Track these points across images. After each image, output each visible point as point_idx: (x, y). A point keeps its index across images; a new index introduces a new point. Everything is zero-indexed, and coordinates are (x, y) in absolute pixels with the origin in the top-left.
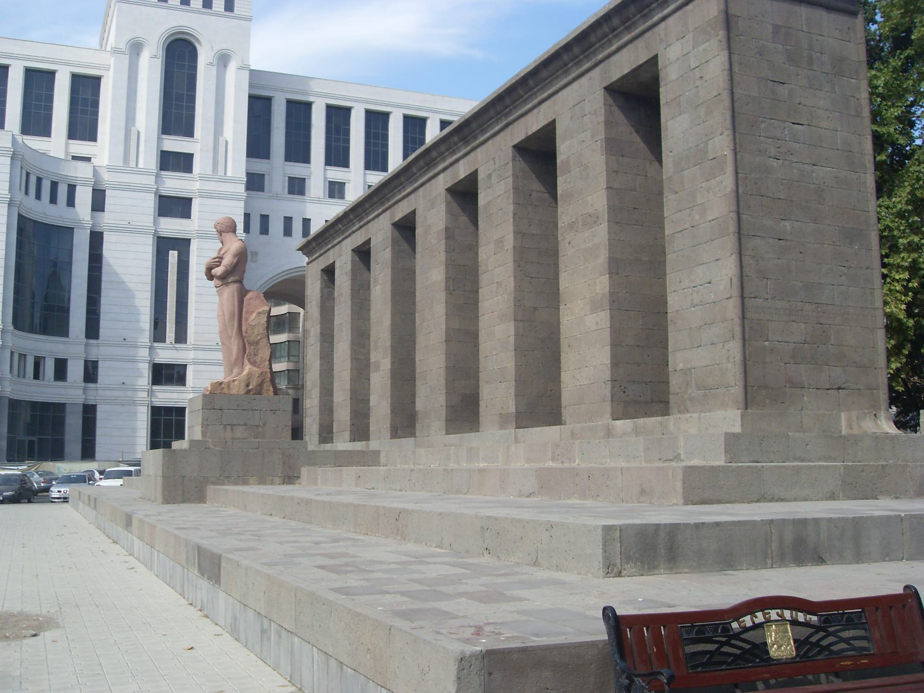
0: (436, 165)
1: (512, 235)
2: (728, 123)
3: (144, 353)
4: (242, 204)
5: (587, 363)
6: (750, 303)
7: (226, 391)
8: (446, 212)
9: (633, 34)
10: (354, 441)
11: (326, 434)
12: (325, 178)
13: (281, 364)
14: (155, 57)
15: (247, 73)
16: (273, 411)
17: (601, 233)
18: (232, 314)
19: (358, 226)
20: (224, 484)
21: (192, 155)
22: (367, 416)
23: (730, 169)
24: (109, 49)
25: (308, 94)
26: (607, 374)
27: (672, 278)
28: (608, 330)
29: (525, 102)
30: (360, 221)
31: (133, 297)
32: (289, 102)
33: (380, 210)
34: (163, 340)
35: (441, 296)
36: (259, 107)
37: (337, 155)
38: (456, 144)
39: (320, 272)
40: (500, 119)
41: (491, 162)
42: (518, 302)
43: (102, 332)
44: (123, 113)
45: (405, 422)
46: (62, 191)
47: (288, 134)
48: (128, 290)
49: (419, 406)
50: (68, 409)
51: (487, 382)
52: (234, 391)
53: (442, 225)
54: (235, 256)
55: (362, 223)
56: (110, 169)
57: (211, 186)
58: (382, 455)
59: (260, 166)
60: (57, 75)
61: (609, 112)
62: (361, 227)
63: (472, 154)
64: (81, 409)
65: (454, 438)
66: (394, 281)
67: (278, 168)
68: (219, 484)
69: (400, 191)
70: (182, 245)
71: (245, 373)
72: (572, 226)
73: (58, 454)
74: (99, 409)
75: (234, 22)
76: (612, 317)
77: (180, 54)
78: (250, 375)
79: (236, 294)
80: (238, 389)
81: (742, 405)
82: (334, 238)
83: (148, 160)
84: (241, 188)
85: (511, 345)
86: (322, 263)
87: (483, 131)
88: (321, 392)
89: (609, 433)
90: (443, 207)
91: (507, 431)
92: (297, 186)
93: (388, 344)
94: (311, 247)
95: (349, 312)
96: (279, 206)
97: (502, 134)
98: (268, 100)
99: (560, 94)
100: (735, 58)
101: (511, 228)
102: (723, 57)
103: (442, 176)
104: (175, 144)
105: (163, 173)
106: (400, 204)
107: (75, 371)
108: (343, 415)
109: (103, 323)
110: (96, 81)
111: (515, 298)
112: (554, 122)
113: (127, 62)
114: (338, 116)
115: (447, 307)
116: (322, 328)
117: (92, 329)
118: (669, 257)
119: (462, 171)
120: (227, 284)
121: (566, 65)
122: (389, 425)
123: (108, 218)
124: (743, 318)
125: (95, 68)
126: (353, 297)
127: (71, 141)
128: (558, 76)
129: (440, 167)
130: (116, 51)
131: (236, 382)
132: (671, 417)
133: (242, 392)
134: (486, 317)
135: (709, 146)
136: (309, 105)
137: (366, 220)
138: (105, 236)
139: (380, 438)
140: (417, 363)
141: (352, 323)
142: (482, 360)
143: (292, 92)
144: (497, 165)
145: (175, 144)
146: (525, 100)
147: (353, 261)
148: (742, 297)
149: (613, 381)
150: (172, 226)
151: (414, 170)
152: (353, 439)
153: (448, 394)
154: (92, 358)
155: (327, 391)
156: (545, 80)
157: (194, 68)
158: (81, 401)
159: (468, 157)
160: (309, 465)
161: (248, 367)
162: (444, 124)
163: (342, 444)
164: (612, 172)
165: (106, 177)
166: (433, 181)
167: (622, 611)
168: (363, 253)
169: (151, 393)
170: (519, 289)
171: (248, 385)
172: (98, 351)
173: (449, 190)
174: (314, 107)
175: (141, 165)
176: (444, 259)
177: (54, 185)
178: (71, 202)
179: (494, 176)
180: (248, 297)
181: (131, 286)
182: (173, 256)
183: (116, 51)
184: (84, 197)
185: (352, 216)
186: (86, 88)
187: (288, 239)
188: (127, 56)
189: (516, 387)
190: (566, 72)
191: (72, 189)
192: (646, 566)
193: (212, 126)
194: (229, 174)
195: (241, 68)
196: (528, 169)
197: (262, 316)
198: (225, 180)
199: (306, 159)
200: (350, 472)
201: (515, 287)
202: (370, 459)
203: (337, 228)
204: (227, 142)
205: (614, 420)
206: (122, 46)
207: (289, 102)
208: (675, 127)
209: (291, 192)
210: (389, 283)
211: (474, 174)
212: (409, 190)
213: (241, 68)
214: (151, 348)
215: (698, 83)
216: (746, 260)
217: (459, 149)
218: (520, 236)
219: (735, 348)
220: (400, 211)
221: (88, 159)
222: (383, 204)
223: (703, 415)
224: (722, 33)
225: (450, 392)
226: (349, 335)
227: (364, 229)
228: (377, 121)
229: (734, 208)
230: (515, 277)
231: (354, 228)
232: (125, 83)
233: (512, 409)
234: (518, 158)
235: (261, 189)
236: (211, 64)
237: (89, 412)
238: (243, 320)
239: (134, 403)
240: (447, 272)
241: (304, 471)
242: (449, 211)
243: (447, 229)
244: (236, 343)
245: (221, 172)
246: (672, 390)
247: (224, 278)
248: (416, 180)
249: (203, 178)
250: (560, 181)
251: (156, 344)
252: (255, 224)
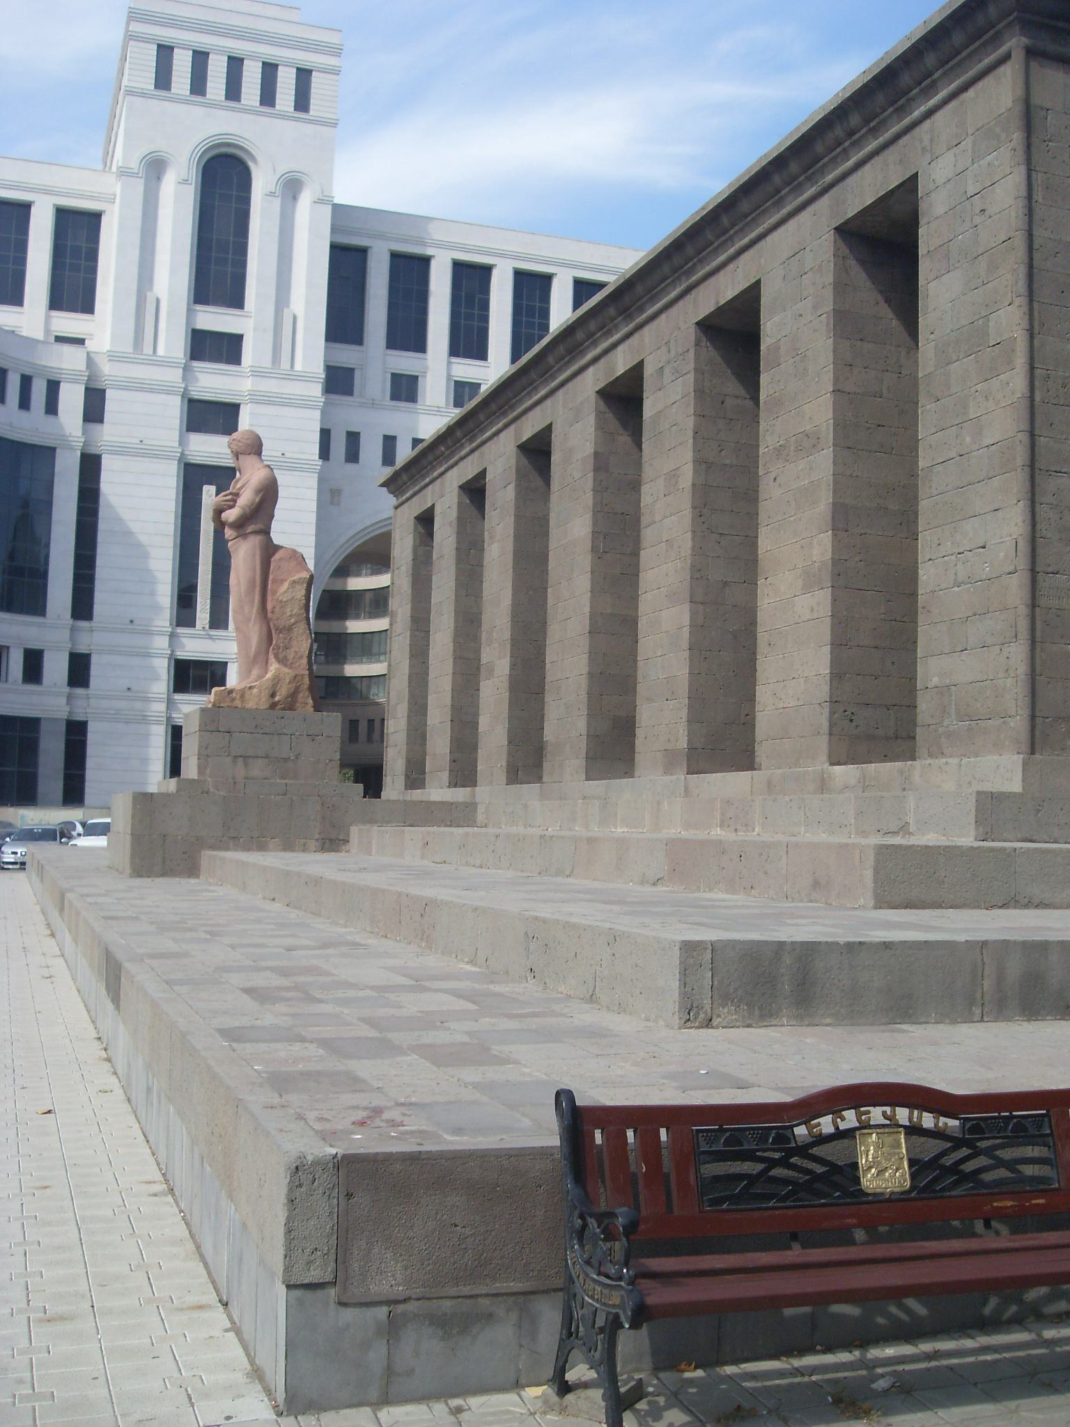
0: (582, 353)
1: (690, 465)
2: (1022, 286)
3: (162, 643)
4: (317, 415)
5: (795, 674)
6: (1045, 582)
7: (238, 703)
8: (597, 429)
9: (881, 140)
10: (455, 786)
11: (416, 776)
12: (449, 377)
13: (379, 665)
14: (185, 182)
15: (328, 210)
16: (312, 737)
17: (822, 464)
18: (252, 583)
19: (468, 449)
20: (227, 849)
21: (239, 338)
22: (474, 748)
23: (1021, 360)
24: (114, 169)
25: (424, 244)
26: (823, 691)
27: (926, 538)
28: (829, 620)
29: (716, 252)
30: (471, 441)
31: (145, 556)
32: (395, 256)
33: (500, 425)
34: (191, 623)
35: (585, 561)
36: (347, 263)
37: (469, 339)
38: (613, 319)
39: (412, 521)
40: (679, 278)
41: (664, 349)
42: (698, 573)
43: (98, 609)
44: (134, 270)
45: (528, 761)
46: (39, 392)
47: (392, 306)
48: (139, 545)
49: (549, 734)
50: (44, 727)
51: (648, 699)
52: (251, 705)
53: (589, 449)
54: (258, 491)
55: (474, 444)
56: (113, 357)
57: (270, 386)
58: (481, 809)
59: (347, 355)
60: (33, 210)
61: (841, 270)
62: (472, 451)
63: (636, 336)
64: (64, 728)
65: (597, 786)
66: (517, 537)
67: (376, 359)
68: (220, 849)
69: (529, 395)
71: (269, 675)
72: (780, 451)
73: (27, 795)
74: (91, 728)
75: (309, 129)
76: (834, 601)
77: (224, 177)
78: (277, 680)
79: (258, 552)
80: (257, 701)
81: (1025, 747)
82: (434, 469)
83: (173, 343)
84: (315, 390)
85: (685, 644)
86: (416, 507)
87: (653, 300)
88: (410, 710)
89: (823, 785)
90: (591, 420)
91: (674, 777)
92: (405, 389)
93: (507, 635)
94: (400, 482)
95: (452, 584)
96: (377, 418)
97: (681, 303)
98: (363, 252)
99: (769, 238)
100: (1039, 178)
101: (689, 455)
102: (1017, 178)
103: (591, 370)
104: (215, 319)
105: (196, 364)
106: (531, 414)
107: (56, 668)
108: (439, 745)
109: (98, 596)
110: (94, 219)
111: (693, 566)
112: (758, 282)
113: (141, 189)
114: (471, 280)
115: (592, 580)
116: (413, 609)
117: (83, 606)
118: (923, 505)
119: (621, 362)
120: (244, 536)
121: (778, 191)
122: (504, 764)
123: (109, 433)
124: (1033, 605)
125: (92, 198)
126: (459, 560)
127: (54, 313)
128: (764, 211)
129: (589, 356)
130: (123, 173)
131: (255, 690)
132: (917, 763)
133: (264, 705)
134: (649, 596)
135: (991, 324)
136: (425, 261)
137: (478, 441)
139: (491, 783)
140: (548, 666)
141: (457, 601)
142: (640, 664)
143: (398, 240)
144: (673, 353)
145: (215, 319)
146: (716, 248)
147: (460, 504)
148: (1033, 571)
149: (834, 702)
151: (551, 360)
152: (454, 784)
153: (591, 716)
154: (82, 649)
155: (418, 708)
156: (746, 216)
157: (246, 201)
158: (64, 715)
159: (628, 342)
160: (364, 822)
161: (274, 667)
162: (583, 289)
163: (438, 791)
164: (843, 366)
165: (107, 369)
166: (579, 378)
167: (591, 1095)
168: (475, 491)
169: (170, 703)
170: (699, 551)
171: (273, 695)
172: (91, 639)
173: (602, 393)
174: (434, 265)
175: (161, 351)
176: (590, 503)
177: (26, 381)
178: (52, 407)
179: (667, 371)
180: (277, 556)
181: (143, 539)
183: (123, 173)
184: (72, 400)
185: (459, 434)
186: (78, 231)
188: (142, 181)
189: (690, 707)
190: (779, 203)
191: (53, 388)
192: (757, 1012)
193: (272, 292)
194: (298, 366)
195: (319, 201)
196: (719, 359)
197: (298, 587)
198: (291, 376)
200: (414, 834)
201: (693, 548)
202: (461, 815)
203: (437, 452)
204: (295, 318)
205: (832, 764)
206: (134, 165)
207: (395, 256)
208: (942, 291)
209: (395, 396)
210: (511, 539)
211: (639, 366)
212: (543, 392)
213: (319, 201)
214: (172, 636)
215: (977, 220)
216: (1042, 511)
217: (616, 328)
218: (704, 467)
219: (1018, 654)
220: (529, 427)
221: (81, 342)
222: (505, 414)
223: (965, 760)
224: (1017, 137)
225: (594, 713)
226: (452, 621)
227: (477, 454)
228: (533, 288)
229: (1025, 426)
230: (694, 532)
231: (463, 453)
232: (138, 224)
233: (683, 743)
234: (704, 342)
235: (349, 391)
236: (272, 194)
237: (76, 733)
238: (269, 592)
239: (144, 720)
240: (595, 524)
241: (354, 831)
242: (600, 426)
243: (596, 454)
244: (257, 628)
245: (285, 364)
246: (919, 720)
247: (240, 525)
248: (553, 377)
249: (257, 373)
250: (764, 379)
251: (180, 630)
252: (339, 446)
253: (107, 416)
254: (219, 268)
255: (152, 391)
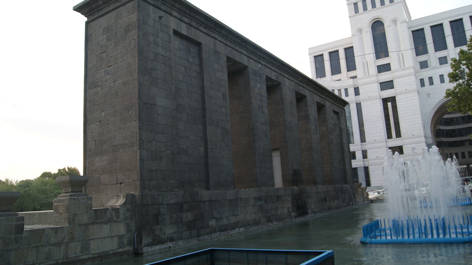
36: (418, 35)
50: (358, 169)
59: (423, 58)
64: (363, 169)
67: (433, 56)
70: (393, 100)
77: (377, 27)
83: (374, 70)
117: (363, 139)
138: (362, 104)
150: (388, 93)
158: (362, 166)
172: (366, 146)
182: (389, 104)
187: (443, 84)
195: (402, 23)
199: (445, 48)
237: (366, 169)
253: (360, 93)
254: (381, 48)
255: (369, 84)
